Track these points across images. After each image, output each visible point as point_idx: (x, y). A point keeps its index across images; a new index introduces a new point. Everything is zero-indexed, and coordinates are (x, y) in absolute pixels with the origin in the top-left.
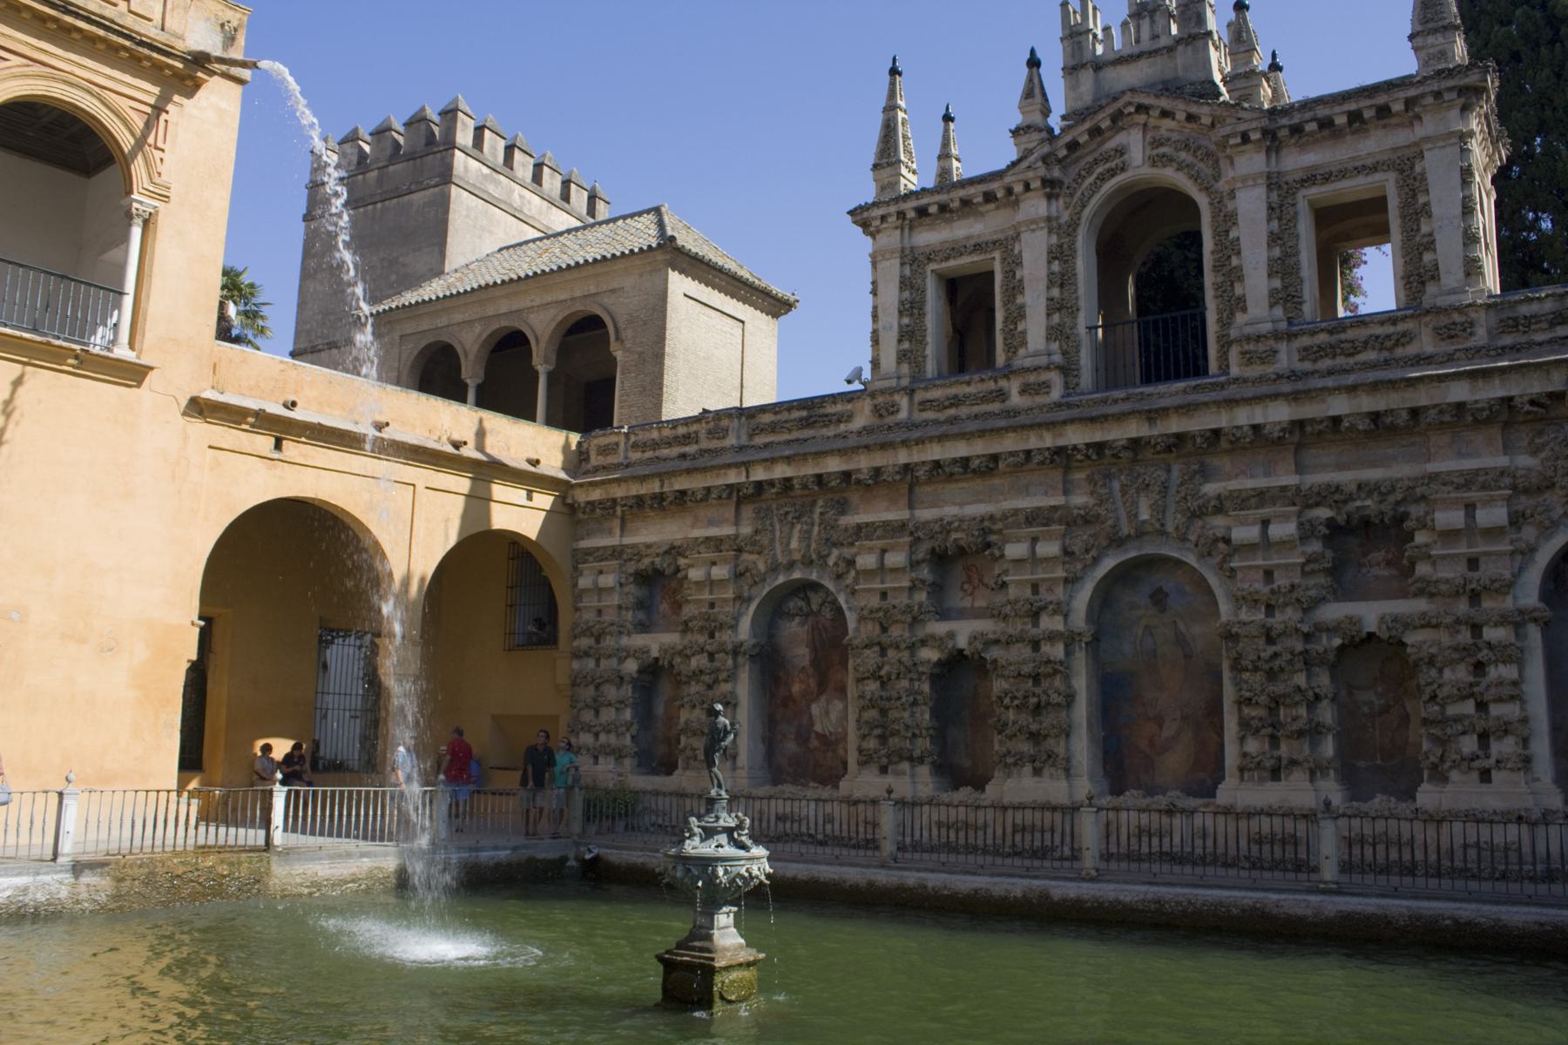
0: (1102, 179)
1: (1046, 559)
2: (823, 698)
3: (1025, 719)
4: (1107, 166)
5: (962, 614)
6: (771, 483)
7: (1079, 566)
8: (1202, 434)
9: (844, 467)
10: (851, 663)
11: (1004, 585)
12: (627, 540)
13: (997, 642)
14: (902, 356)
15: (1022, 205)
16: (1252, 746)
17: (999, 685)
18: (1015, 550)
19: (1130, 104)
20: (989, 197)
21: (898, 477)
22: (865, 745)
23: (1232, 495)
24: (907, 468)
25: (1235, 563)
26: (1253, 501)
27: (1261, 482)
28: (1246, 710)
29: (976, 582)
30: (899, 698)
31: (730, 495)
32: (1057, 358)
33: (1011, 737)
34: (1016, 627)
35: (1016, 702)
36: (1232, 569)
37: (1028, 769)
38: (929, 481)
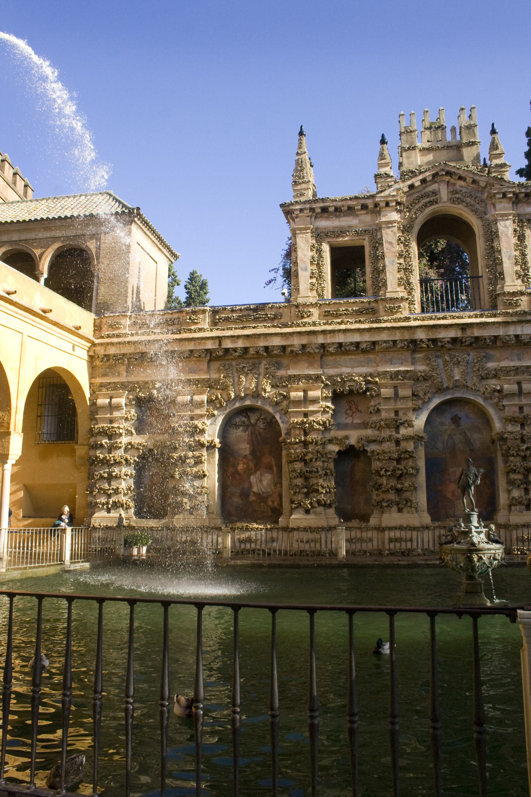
0: (426, 206)
1: (403, 398)
2: (258, 473)
3: (393, 483)
4: (428, 199)
5: (346, 427)
6: (235, 350)
7: (420, 402)
8: (490, 337)
9: (284, 343)
10: (284, 452)
11: (378, 411)
12: (132, 379)
13: (374, 441)
14: (312, 284)
15: (382, 214)
16: (516, 493)
17: (376, 465)
18: (386, 392)
19: (443, 170)
20: (364, 207)
21: (317, 351)
22: (295, 498)
23: (502, 369)
24: (323, 346)
25: (505, 402)
26: (512, 373)
27: (518, 364)
28: (512, 476)
29: (354, 410)
30: (318, 472)
31: (206, 354)
32: (405, 295)
33: (384, 492)
34: (386, 433)
35: (389, 473)
36: (504, 406)
37: (395, 508)
38: (332, 354)
